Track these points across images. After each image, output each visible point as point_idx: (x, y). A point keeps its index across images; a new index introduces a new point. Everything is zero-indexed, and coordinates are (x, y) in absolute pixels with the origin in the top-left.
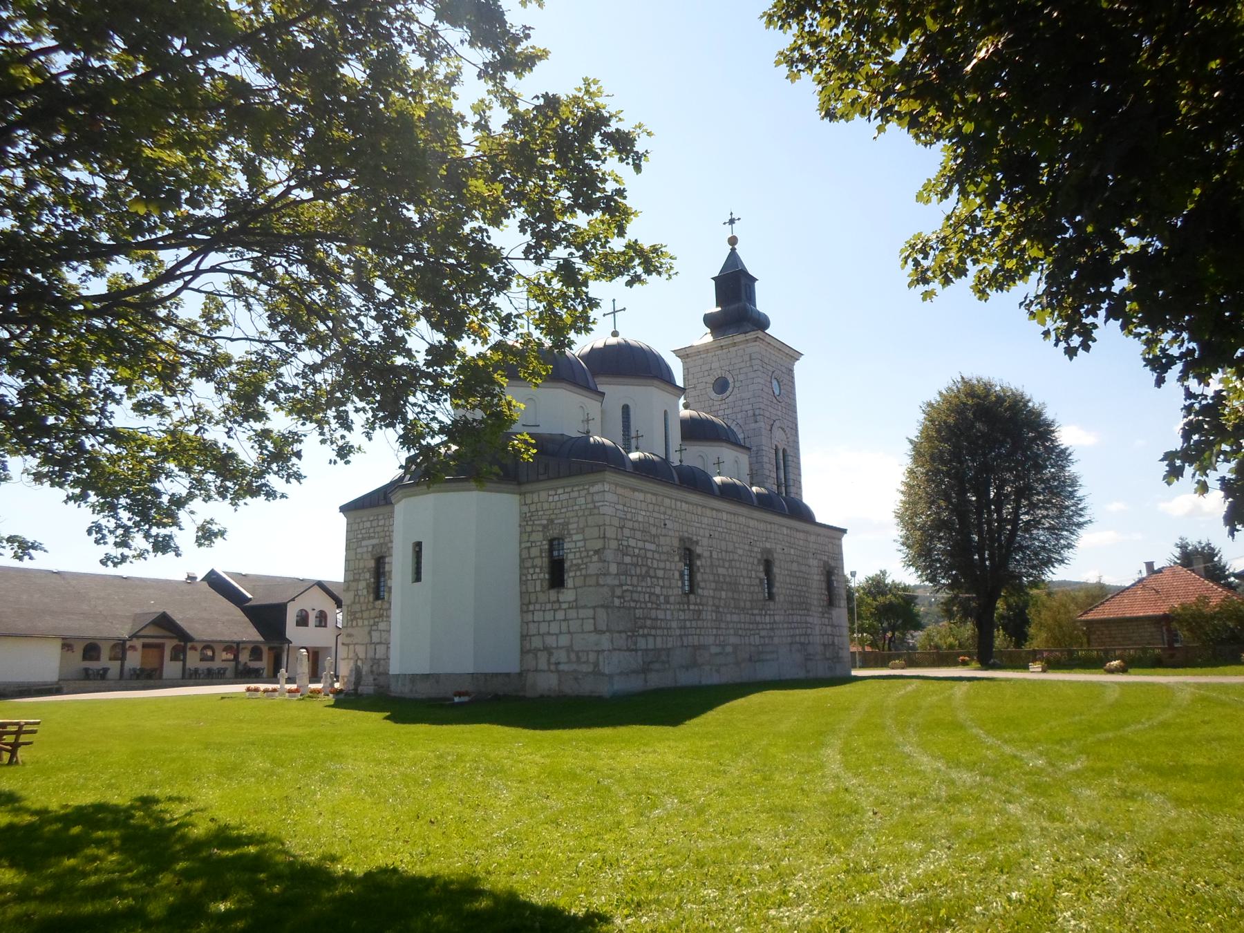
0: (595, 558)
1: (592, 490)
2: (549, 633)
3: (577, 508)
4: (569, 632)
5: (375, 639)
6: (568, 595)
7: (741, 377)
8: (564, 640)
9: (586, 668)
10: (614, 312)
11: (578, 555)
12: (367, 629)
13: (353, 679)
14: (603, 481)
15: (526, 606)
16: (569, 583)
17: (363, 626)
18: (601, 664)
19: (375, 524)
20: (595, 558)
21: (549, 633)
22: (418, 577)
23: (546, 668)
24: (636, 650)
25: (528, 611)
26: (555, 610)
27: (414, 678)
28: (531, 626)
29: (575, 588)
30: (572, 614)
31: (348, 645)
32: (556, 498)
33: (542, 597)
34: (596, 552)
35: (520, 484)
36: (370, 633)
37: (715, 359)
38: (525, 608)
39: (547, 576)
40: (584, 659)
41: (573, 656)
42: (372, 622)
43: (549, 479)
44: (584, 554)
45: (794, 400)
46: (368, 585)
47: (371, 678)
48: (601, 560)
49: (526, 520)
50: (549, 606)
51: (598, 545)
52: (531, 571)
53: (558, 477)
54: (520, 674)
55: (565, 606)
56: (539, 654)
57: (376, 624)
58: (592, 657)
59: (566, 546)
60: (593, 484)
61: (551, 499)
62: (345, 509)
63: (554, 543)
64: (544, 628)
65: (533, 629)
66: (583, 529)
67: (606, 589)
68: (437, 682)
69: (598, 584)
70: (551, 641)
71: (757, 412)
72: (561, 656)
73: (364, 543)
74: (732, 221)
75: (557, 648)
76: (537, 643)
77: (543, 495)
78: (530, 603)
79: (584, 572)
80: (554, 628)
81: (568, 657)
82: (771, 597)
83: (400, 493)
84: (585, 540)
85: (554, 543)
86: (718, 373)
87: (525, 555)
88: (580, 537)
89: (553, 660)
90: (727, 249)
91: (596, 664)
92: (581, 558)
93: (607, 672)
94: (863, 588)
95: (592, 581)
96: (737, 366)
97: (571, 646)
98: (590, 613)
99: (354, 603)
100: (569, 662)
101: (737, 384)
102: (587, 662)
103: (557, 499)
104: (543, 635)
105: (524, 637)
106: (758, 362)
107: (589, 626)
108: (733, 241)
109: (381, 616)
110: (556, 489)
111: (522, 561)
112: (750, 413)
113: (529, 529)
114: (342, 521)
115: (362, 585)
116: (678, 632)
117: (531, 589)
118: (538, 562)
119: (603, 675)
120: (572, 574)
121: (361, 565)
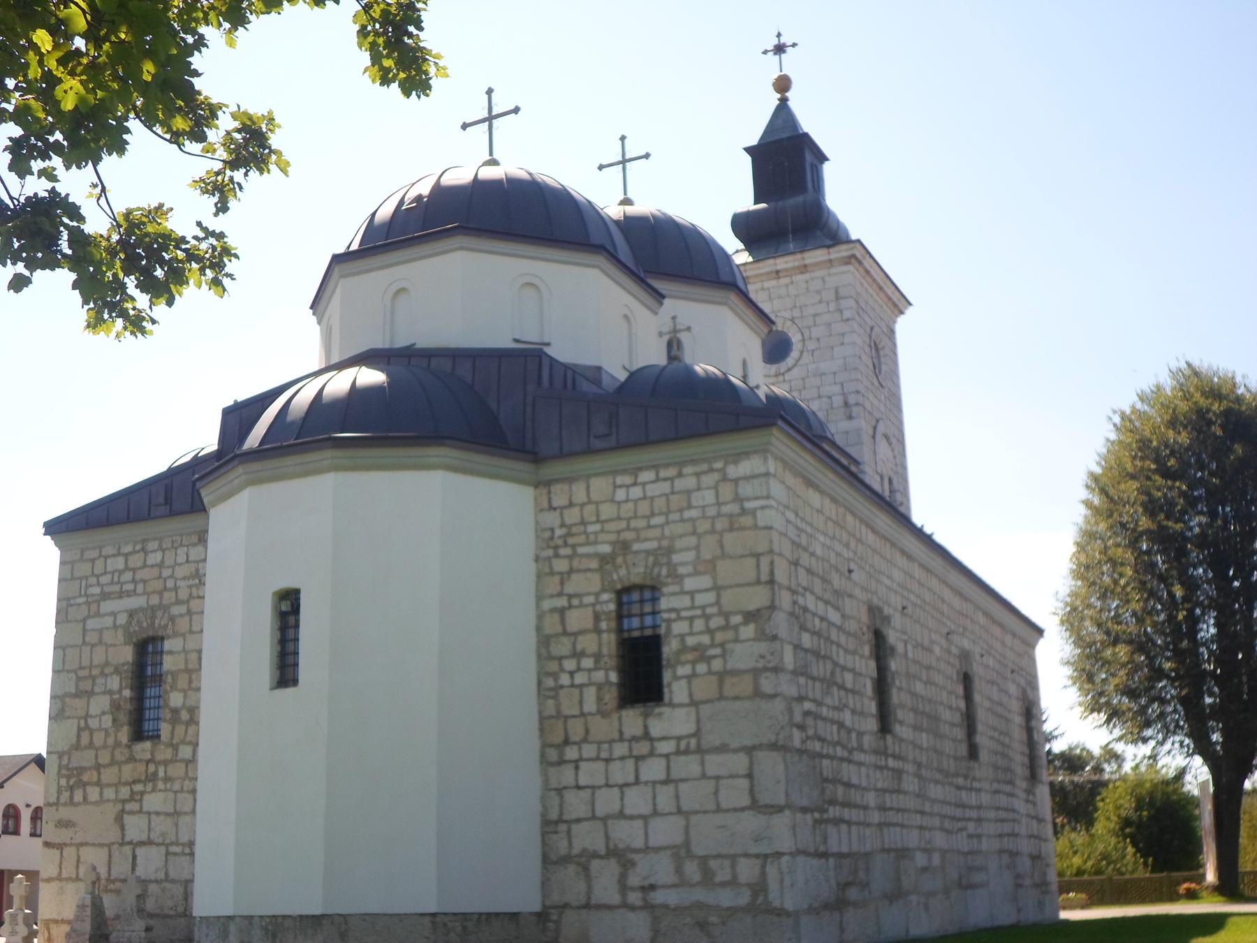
1: (732, 471)
3: (693, 513)
4: (679, 811)
5: (133, 834)
6: (672, 721)
7: (817, 332)
8: (666, 831)
9: (726, 898)
10: (624, 162)
11: (699, 625)
12: (111, 810)
13: (87, 927)
14: (763, 451)
15: (555, 748)
16: (677, 690)
17: (102, 801)
18: (773, 886)
19: (136, 561)
20: (748, 631)
21: (621, 815)
22: (286, 671)
23: (616, 899)
24: (824, 855)
25: (562, 762)
26: (639, 759)
28: (570, 796)
29: (694, 703)
30: (688, 766)
31: (60, 847)
32: (636, 492)
33: (602, 728)
34: (750, 617)
35: (536, 458)
36: (119, 819)
38: (553, 755)
39: (614, 677)
40: (723, 875)
42: (125, 792)
43: (620, 447)
44: (716, 622)
45: (898, 386)
46: (116, 707)
47: (139, 925)
48: (762, 636)
49: (553, 547)
50: (620, 749)
51: (757, 598)
52: (570, 665)
53: (644, 442)
54: (542, 916)
55: (665, 747)
56: (595, 864)
57: (136, 797)
58: (747, 871)
59: (664, 604)
60: (737, 457)
61: (621, 495)
62: (57, 528)
63: (635, 597)
64: (607, 802)
65: (576, 804)
66: (712, 563)
67: (778, 705)
68: (343, 935)
69: (758, 694)
70: (628, 834)
71: (852, 399)
72: (661, 869)
73: (107, 606)
74: (780, 49)
75: (647, 849)
76: (587, 838)
77: (600, 486)
78: (567, 742)
79: (717, 665)
80: (637, 801)
81: (679, 870)
82: (973, 752)
83: (238, 473)
84: (717, 589)
85: (635, 597)
87: (552, 625)
88: (705, 581)
89: (634, 880)
90: (774, 99)
91: (759, 888)
92: (710, 631)
93: (789, 905)
95: (744, 685)
96: (810, 311)
97: (687, 843)
98: (740, 762)
99: (77, 747)
100: (682, 883)
101: (811, 345)
102: (733, 882)
103: (628, 496)
104: (605, 819)
105: (549, 826)
106: (852, 303)
107: (735, 793)
108: (783, 85)
109: (153, 778)
110: (636, 471)
111: (544, 641)
112: (838, 401)
113: (561, 565)
114: (49, 554)
115: (100, 704)
116: (876, 817)
117: (569, 708)
118: (588, 643)
119: (781, 912)
120: (682, 670)
121: (99, 657)
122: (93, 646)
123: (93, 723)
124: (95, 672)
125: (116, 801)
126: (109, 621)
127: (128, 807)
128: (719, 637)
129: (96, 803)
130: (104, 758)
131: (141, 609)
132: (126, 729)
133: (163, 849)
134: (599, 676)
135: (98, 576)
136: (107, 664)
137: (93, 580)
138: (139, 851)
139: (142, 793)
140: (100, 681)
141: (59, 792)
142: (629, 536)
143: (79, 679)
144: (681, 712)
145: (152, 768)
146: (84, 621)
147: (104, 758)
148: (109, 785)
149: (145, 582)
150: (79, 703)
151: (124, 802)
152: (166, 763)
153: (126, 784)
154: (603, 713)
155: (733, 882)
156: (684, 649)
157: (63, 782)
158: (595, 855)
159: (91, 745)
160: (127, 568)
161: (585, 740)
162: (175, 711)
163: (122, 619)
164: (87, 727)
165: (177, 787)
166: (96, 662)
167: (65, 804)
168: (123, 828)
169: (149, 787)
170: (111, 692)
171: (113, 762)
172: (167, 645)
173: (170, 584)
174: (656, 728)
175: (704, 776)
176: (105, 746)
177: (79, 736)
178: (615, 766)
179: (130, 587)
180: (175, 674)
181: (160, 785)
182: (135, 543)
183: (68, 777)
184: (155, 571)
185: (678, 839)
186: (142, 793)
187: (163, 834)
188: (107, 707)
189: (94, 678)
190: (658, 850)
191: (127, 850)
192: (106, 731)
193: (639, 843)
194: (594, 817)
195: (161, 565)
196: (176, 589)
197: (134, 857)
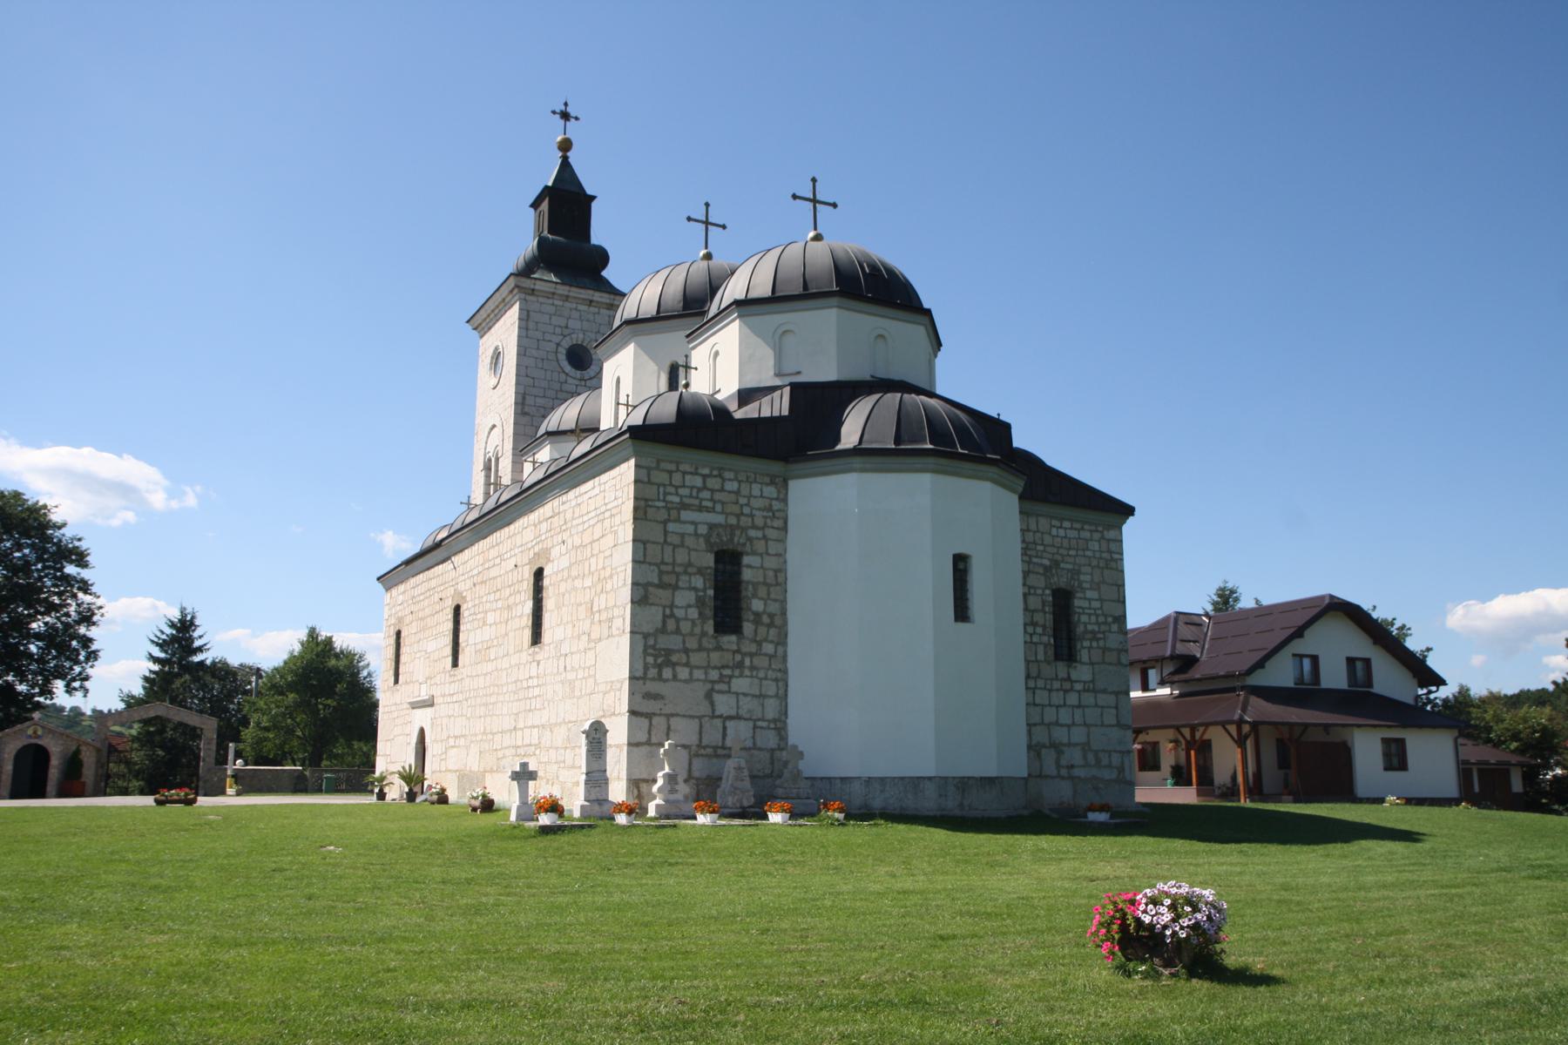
0: (1115, 627)
2: (1057, 724)
3: (1088, 553)
6: (1082, 673)
8: (1078, 735)
9: (1108, 775)
16: (1084, 655)
19: (711, 483)
20: (1115, 627)
21: (1057, 724)
22: (962, 612)
23: (1055, 773)
26: (1066, 691)
27: (964, 784)
30: (1088, 699)
31: (649, 716)
36: (709, 696)
37: (575, 314)
40: (1105, 762)
41: (1091, 757)
42: (714, 675)
44: (1101, 619)
46: (700, 602)
50: (1056, 685)
55: (1078, 687)
58: (1116, 759)
72: (1074, 756)
73: (685, 515)
75: (1069, 745)
79: (1101, 643)
81: (1085, 757)
86: (578, 338)
92: (1097, 623)
94: (292, 671)
99: (663, 630)
100: (1086, 765)
102: (1110, 766)
104: (1049, 725)
108: (566, 146)
110: (1062, 520)
115: (684, 598)
120: (1086, 644)
121: (681, 557)
122: (675, 547)
123: (679, 613)
124: (677, 569)
125: (706, 681)
126: (690, 529)
127: (717, 687)
128: (1103, 628)
129: (685, 681)
130: (692, 643)
131: (719, 525)
132: (711, 622)
133: (751, 724)
134: (1045, 639)
135: (677, 487)
136: (690, 564)
137: (673, 490)
138: (728, 724)
139: (731, 677)
140: (684, 578)
141: (646, 668)
142: (1059, 558)
143: (661, 573)
144: (1085, 668)
145: (738, 657)
146: (665, 523)
147: (692, 643)
148: (698, 667)
149: (723, 504)
150: (664, 595)
151: (713, 682)
152: (751, 655)
153: (715, 668)
154: (1047, 661)
155: (1110, 766)
156: (1086, 631)
157: (650, 660)
158: (1044, 746)
159: (678, 631)
160: (705, 488)
161: (1038, 676)
162: (757, 615)
163: (703, 530)
164: (672, 615)
165: (761, 674)
166: (679, 560)
167: (653, 679)
168: (712, 704)
169: (737, 672)
170: (695, 589)
171: (700, 649)
172: (746, 560)
173: (746, 510)
174: (1074, 676)
175: (1096, 705)
176: (692, 634)
177: (664, 622)
178: (1054, 694)
179: (709, 504)
180: (755, 585)
181: (747, 672)
182: (712, 469)
183: (656, 657)
184: (733, 497)
185: (1083, 739)
186: (731, 677)
187: (749, 711)
188: (693, 601)
189: (678, 575)
190: (1076, 745)
191: (718, 722)
192: (693, 622)
193: (1065, 741)
194: (1042, 723)
195: (738, 493)
196: (752, 516)
197: (725, 728)
